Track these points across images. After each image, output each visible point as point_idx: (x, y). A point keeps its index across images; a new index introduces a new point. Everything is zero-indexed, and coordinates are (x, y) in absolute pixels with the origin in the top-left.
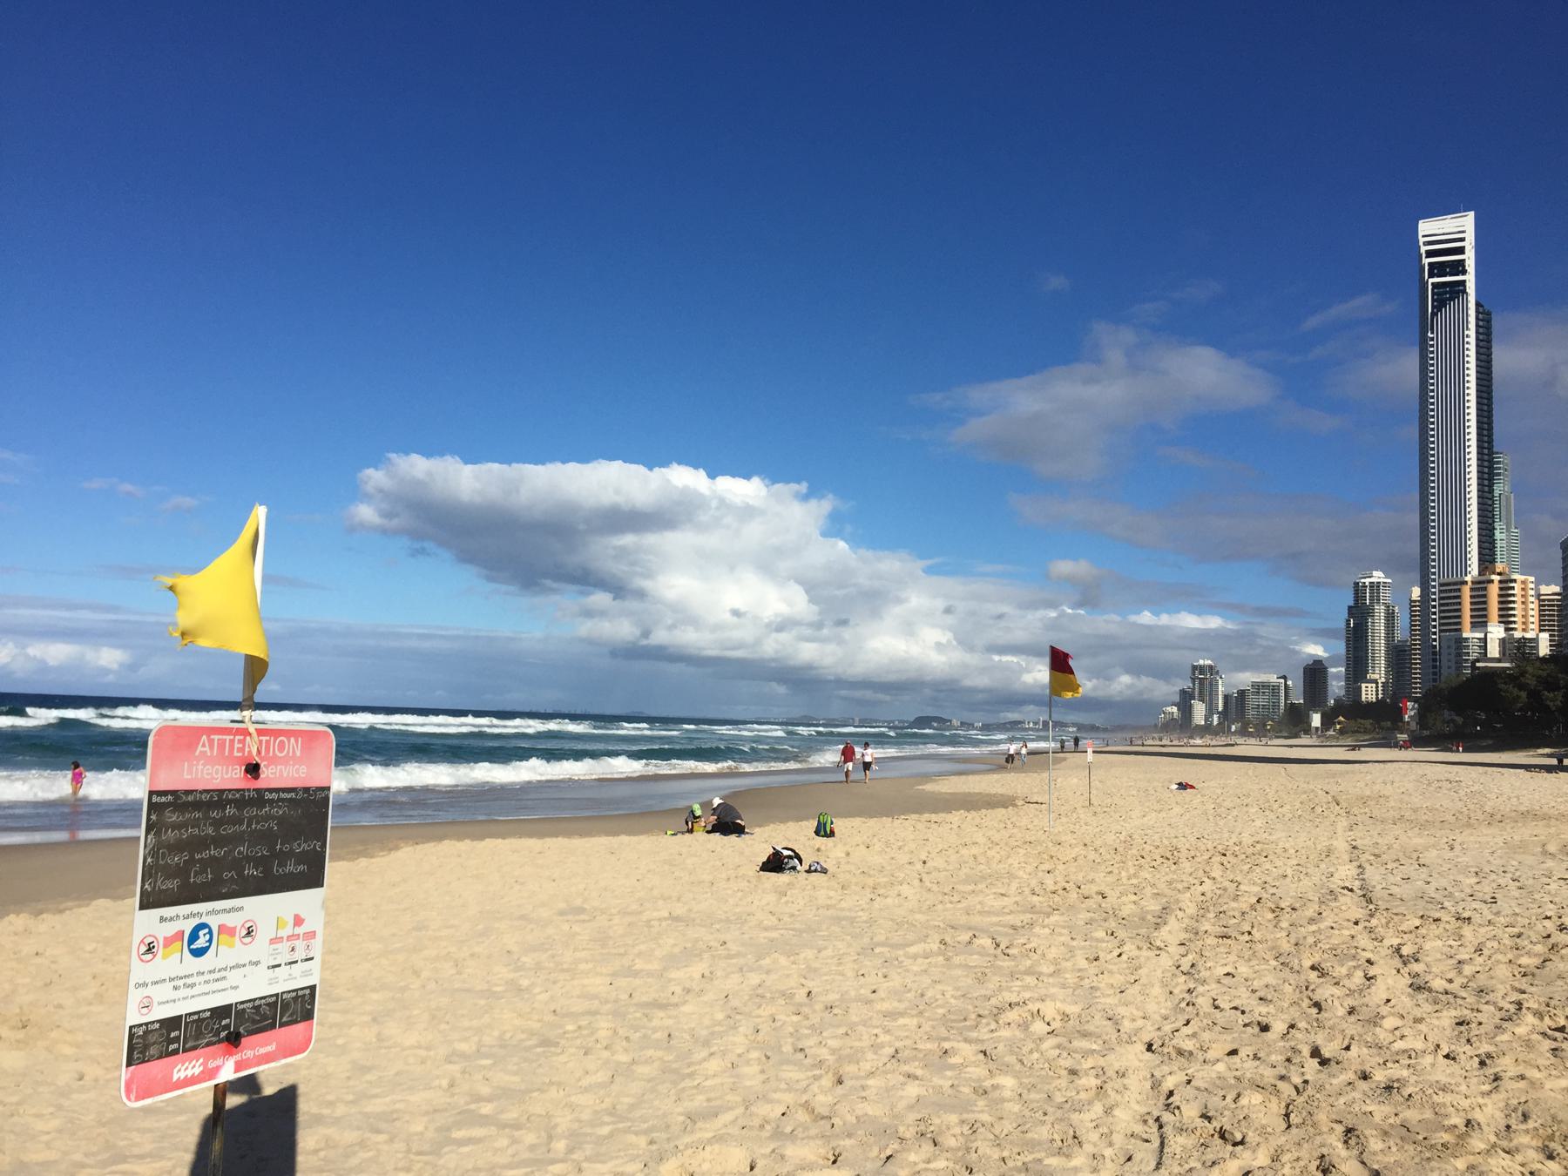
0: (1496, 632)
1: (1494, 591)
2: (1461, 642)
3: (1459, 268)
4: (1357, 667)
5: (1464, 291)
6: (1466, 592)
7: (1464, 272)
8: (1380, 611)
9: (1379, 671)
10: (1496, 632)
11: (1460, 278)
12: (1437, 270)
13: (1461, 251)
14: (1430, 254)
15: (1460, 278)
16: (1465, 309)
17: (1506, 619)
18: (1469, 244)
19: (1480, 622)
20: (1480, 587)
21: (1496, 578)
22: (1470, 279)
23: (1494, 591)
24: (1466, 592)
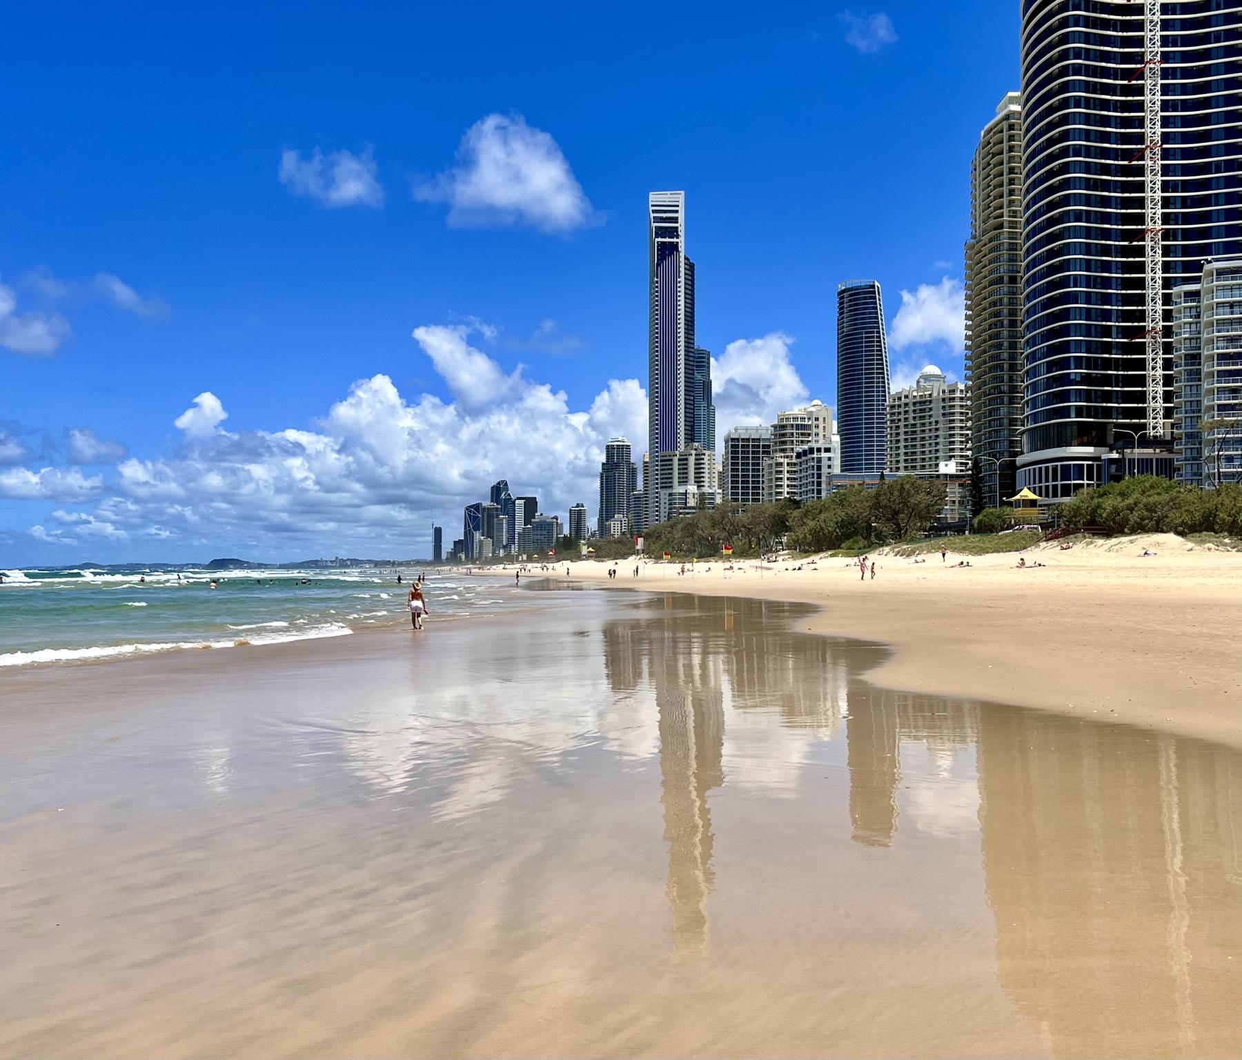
1: (692, 460)
3: (673, 232)
5: (677, 251)
6: (676, 460)
7: (678, 237)
11: (675, 240)
12: (661, 232)
13: (675, 220)
14: (657, 220)
15: (675, 240)
17: (699, 482)
18: (681, 216)
20: (684, 460)
21: (694, 452)
22: (681, 241)
23: (692, 460)
24: (676, 460)
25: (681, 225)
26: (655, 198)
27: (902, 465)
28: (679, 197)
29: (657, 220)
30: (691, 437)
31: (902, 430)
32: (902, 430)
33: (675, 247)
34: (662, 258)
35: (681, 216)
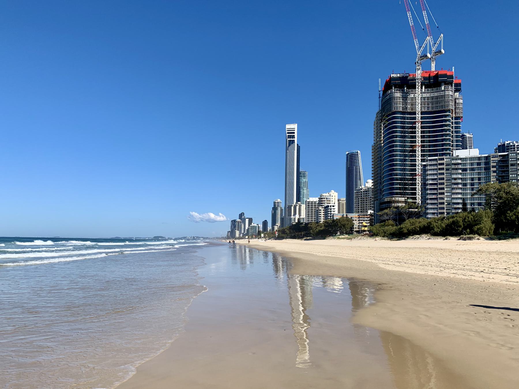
0: (297, 216)
1: (298, 207)
2: (291, 219)
3: (293, 137)
4: (274, 223)
6: (292, 208)
8: (279, 209)
9: (278, 224)
10: (297, 216)
12: (290, 137)
13: (294, 133)
14: (288, 133)
16: (294, 146)
18: (296, 132)
19: (295, 214)
22: (296, 139)
23: (298, 207)
24: (292, 208)
25: (296, 135)
26: (288, 126)
27: (360, 210)
28: (295, 126)
29: (288, 133)
30: (298, 199)
31: (360, 200)
32: (360, 200)
33: (293, 142)
34: (289, 145)
35: (296, 132)
